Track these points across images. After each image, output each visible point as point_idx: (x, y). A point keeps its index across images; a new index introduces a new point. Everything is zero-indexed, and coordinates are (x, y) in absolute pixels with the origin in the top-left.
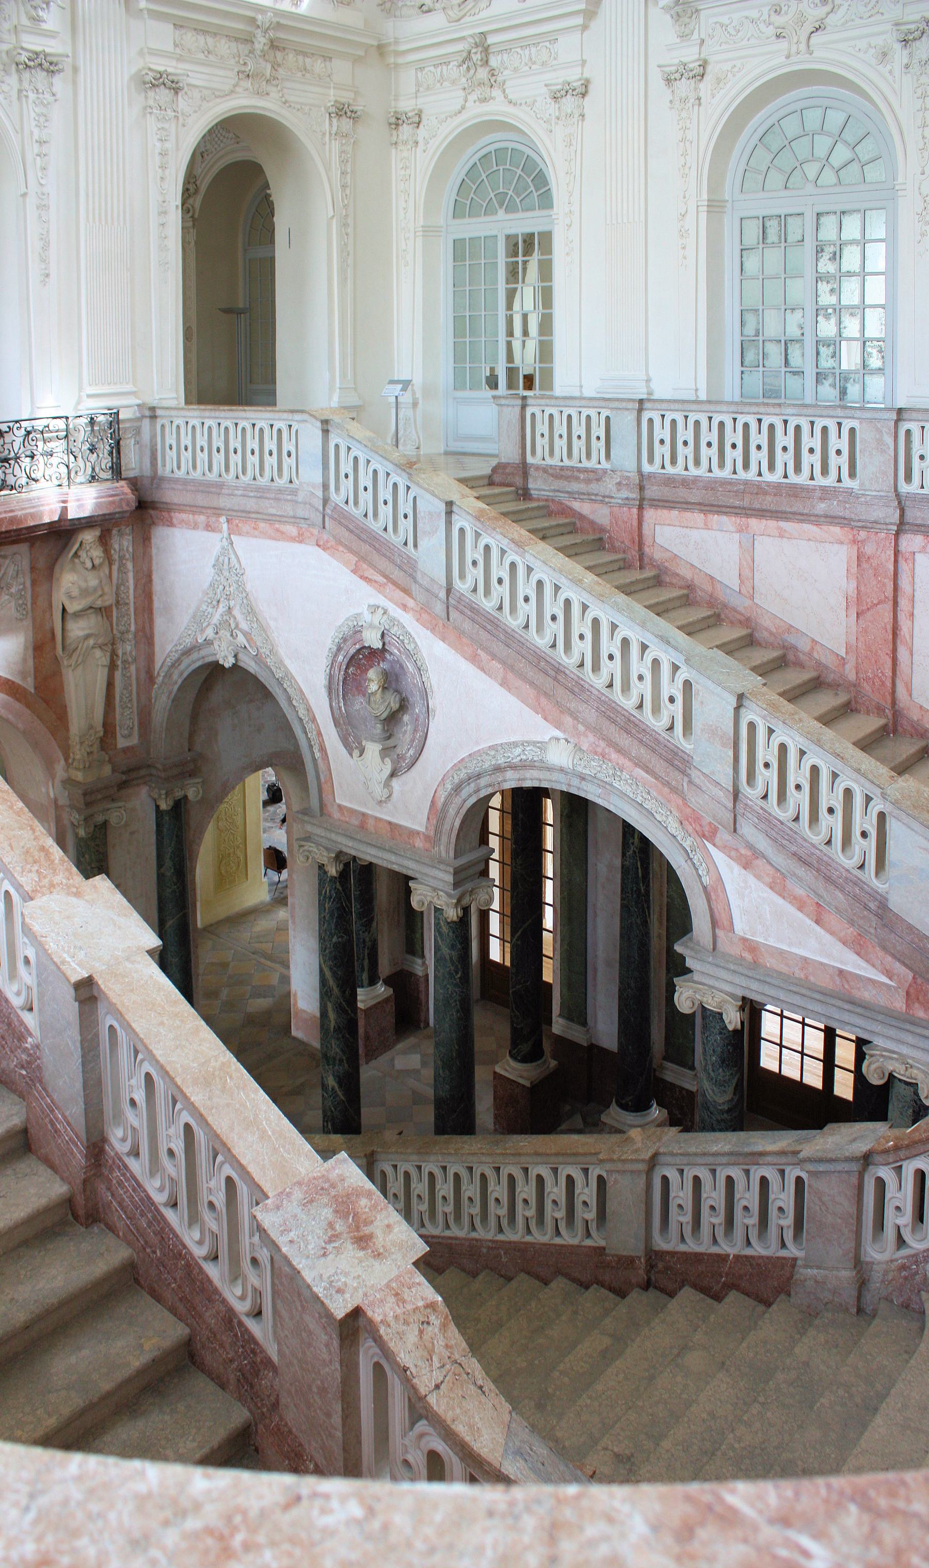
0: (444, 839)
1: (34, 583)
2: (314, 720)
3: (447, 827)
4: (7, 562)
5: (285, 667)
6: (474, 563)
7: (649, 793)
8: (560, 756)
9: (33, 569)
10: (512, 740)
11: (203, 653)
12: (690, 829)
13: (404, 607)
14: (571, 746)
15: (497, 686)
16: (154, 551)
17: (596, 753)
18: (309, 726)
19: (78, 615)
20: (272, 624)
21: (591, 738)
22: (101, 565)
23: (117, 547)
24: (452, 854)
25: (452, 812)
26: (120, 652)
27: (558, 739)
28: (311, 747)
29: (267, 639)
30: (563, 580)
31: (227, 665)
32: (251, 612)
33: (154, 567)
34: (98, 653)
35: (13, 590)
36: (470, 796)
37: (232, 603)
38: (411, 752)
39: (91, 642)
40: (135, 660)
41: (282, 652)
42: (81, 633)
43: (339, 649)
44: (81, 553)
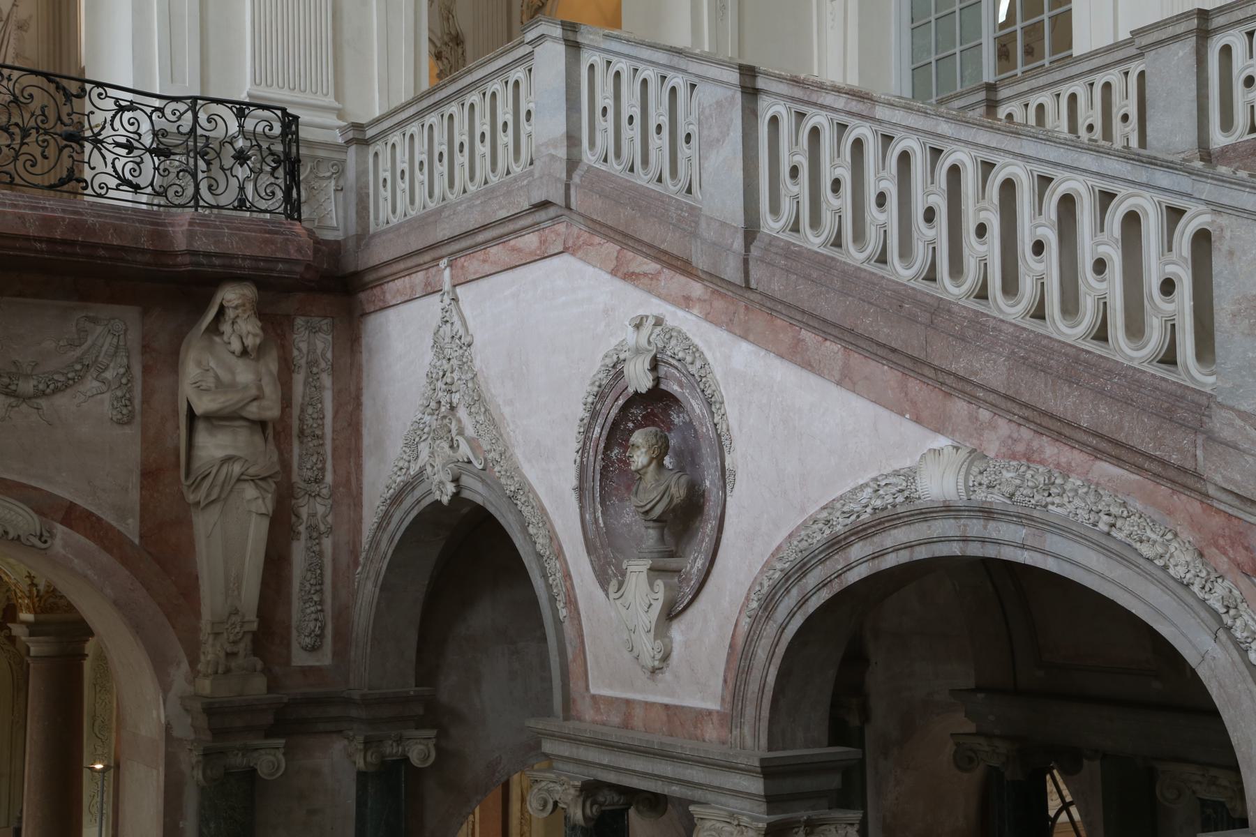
0: (750, 711)
1: (146, 370)
2: (560, 554)
3: (753, 687)
4: (99, 329)
5: (522, 476)
6: (794, 172)
7: (1124, 504)
8: (940, 484)
9: (146, 348)
10: (861, 482)
11: (418, 493)
12: (1223, 563)
13: (686, 302)
14: (963, 453)
15: (834, 391)
16: (365, 356)
17: (1013, 457)
18: (554, 565)
19: (216, 419)
20: (506, 410)
21: (1004, 427)
22: (261, 350)
23: (304, 346)
24: (764, 741)
25: (761, 654)
26: (304, 512)
27: (938, 452)
28: (553, 599)
29: (498, 438)
30: (944, 128)
31: (445, 500)
32: (478, 400)
33: (364, 384)
34: (250, 491)
35: (108, 375)
36: (792, 615)
37: (456, 398)
38: (699, 563)
39: (237, 468)
40: (330, 530)
41: (519, 454)
42: (220, 454)
43: (594, 415)
44: (226, 327)
